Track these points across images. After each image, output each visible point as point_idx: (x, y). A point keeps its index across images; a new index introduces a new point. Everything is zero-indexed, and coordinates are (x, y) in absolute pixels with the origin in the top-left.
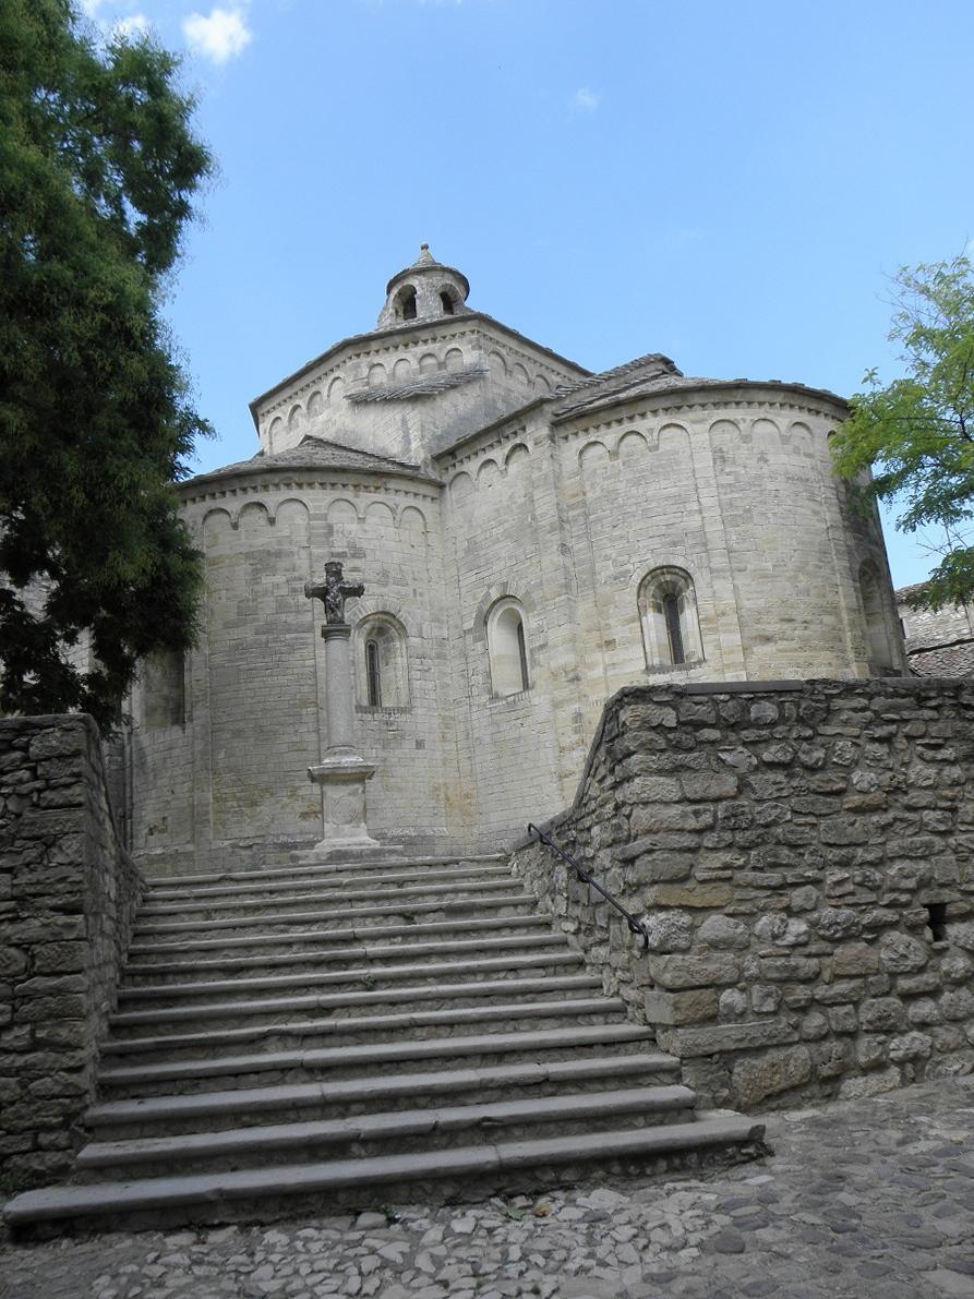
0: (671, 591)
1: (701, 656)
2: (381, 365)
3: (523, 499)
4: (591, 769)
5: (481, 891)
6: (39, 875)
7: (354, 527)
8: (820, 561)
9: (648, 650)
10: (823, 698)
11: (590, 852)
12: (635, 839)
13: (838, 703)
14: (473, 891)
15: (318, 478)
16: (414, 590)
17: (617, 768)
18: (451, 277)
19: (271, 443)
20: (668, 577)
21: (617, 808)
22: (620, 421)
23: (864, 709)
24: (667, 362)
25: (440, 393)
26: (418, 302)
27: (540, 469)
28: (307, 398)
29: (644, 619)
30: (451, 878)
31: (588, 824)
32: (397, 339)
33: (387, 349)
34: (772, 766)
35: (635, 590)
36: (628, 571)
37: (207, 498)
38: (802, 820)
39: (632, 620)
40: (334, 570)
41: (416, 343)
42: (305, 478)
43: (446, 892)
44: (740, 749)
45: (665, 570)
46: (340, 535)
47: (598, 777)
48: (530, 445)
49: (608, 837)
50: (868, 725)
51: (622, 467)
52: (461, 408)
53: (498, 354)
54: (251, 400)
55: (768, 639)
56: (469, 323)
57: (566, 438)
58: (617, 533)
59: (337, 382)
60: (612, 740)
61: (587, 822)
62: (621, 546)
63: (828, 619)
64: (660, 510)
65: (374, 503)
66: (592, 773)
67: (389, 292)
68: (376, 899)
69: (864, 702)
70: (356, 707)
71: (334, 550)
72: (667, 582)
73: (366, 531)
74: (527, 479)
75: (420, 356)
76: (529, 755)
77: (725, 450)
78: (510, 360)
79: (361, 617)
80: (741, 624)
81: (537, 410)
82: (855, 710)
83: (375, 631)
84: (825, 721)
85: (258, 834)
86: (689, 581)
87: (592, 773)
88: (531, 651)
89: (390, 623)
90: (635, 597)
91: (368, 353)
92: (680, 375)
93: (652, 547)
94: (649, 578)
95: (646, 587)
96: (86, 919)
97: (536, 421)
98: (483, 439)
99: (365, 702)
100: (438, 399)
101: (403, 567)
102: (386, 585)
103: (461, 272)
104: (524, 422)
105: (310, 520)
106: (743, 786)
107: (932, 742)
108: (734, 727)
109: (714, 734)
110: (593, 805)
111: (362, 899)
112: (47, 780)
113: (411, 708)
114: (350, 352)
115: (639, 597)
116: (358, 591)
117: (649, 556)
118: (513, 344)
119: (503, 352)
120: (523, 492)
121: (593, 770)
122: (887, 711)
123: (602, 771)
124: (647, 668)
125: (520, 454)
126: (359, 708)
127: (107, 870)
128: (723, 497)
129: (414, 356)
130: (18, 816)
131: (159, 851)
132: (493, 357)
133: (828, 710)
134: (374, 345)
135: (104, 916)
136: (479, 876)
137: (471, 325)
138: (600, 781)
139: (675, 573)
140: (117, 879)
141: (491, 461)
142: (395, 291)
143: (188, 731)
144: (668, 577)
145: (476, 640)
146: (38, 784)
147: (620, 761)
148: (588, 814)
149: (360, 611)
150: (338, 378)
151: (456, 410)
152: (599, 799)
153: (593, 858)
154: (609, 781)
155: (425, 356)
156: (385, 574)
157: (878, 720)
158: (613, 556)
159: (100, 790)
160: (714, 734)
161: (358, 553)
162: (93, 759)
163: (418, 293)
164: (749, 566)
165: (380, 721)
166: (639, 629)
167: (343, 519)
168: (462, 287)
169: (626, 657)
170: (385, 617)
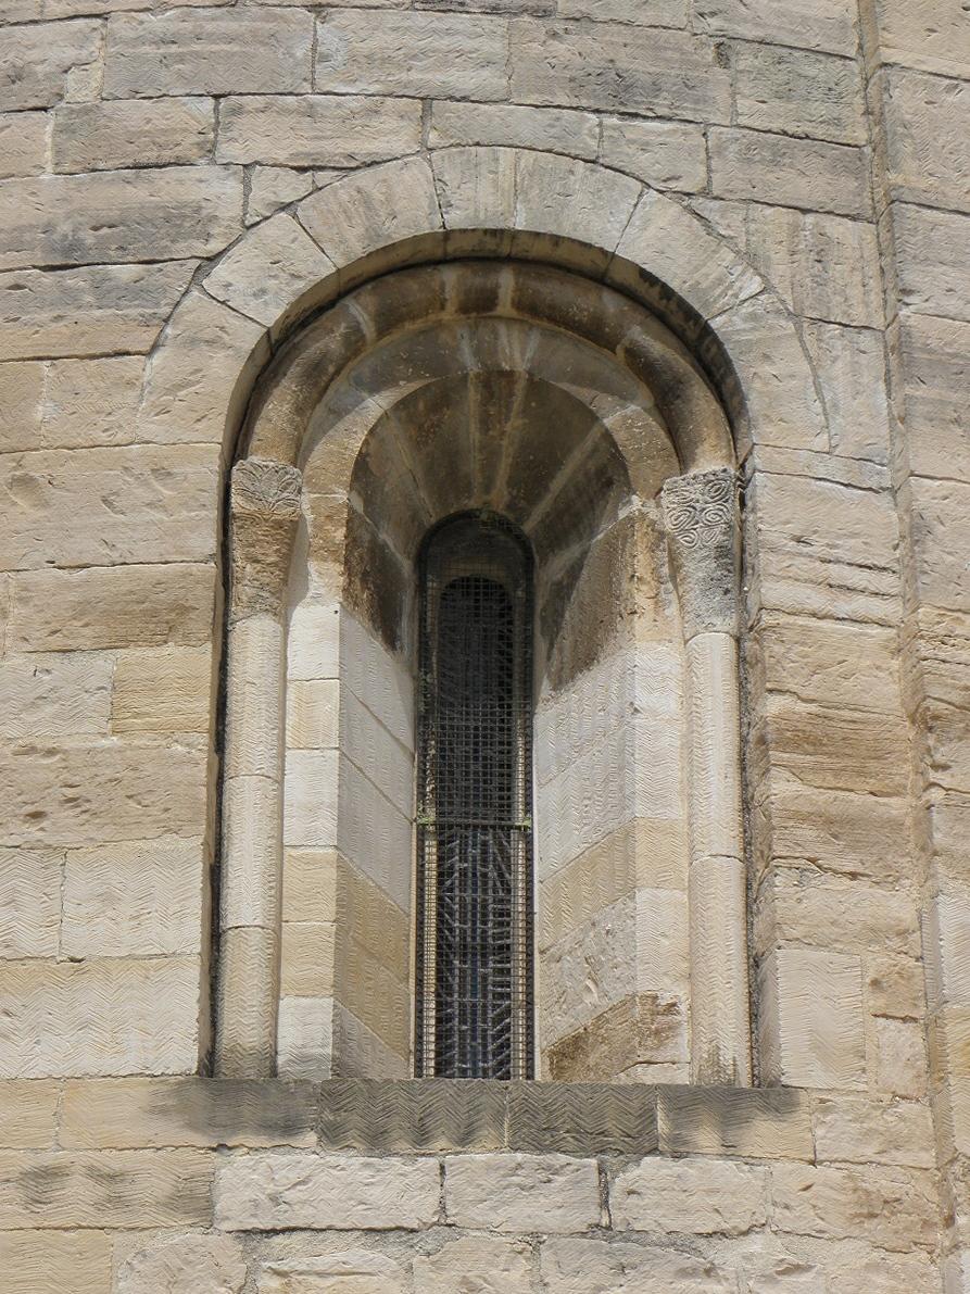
0: (500, 497)
1: (734, 1049)
9: (245, 904)
20: (518, 350)
29: (253, 635)
35: (224, 373)
36: (188, 219)
45: (506, 282)
72: (496, 381)
86: (701, 403)
90: (213, 434)
94: (360, 311)
95: (319, 381)
115: (237, 445)
117: (392, 134)
124: (210, 1064)
144: (518, 350)
158: (81, 89)
166: (204, 706)
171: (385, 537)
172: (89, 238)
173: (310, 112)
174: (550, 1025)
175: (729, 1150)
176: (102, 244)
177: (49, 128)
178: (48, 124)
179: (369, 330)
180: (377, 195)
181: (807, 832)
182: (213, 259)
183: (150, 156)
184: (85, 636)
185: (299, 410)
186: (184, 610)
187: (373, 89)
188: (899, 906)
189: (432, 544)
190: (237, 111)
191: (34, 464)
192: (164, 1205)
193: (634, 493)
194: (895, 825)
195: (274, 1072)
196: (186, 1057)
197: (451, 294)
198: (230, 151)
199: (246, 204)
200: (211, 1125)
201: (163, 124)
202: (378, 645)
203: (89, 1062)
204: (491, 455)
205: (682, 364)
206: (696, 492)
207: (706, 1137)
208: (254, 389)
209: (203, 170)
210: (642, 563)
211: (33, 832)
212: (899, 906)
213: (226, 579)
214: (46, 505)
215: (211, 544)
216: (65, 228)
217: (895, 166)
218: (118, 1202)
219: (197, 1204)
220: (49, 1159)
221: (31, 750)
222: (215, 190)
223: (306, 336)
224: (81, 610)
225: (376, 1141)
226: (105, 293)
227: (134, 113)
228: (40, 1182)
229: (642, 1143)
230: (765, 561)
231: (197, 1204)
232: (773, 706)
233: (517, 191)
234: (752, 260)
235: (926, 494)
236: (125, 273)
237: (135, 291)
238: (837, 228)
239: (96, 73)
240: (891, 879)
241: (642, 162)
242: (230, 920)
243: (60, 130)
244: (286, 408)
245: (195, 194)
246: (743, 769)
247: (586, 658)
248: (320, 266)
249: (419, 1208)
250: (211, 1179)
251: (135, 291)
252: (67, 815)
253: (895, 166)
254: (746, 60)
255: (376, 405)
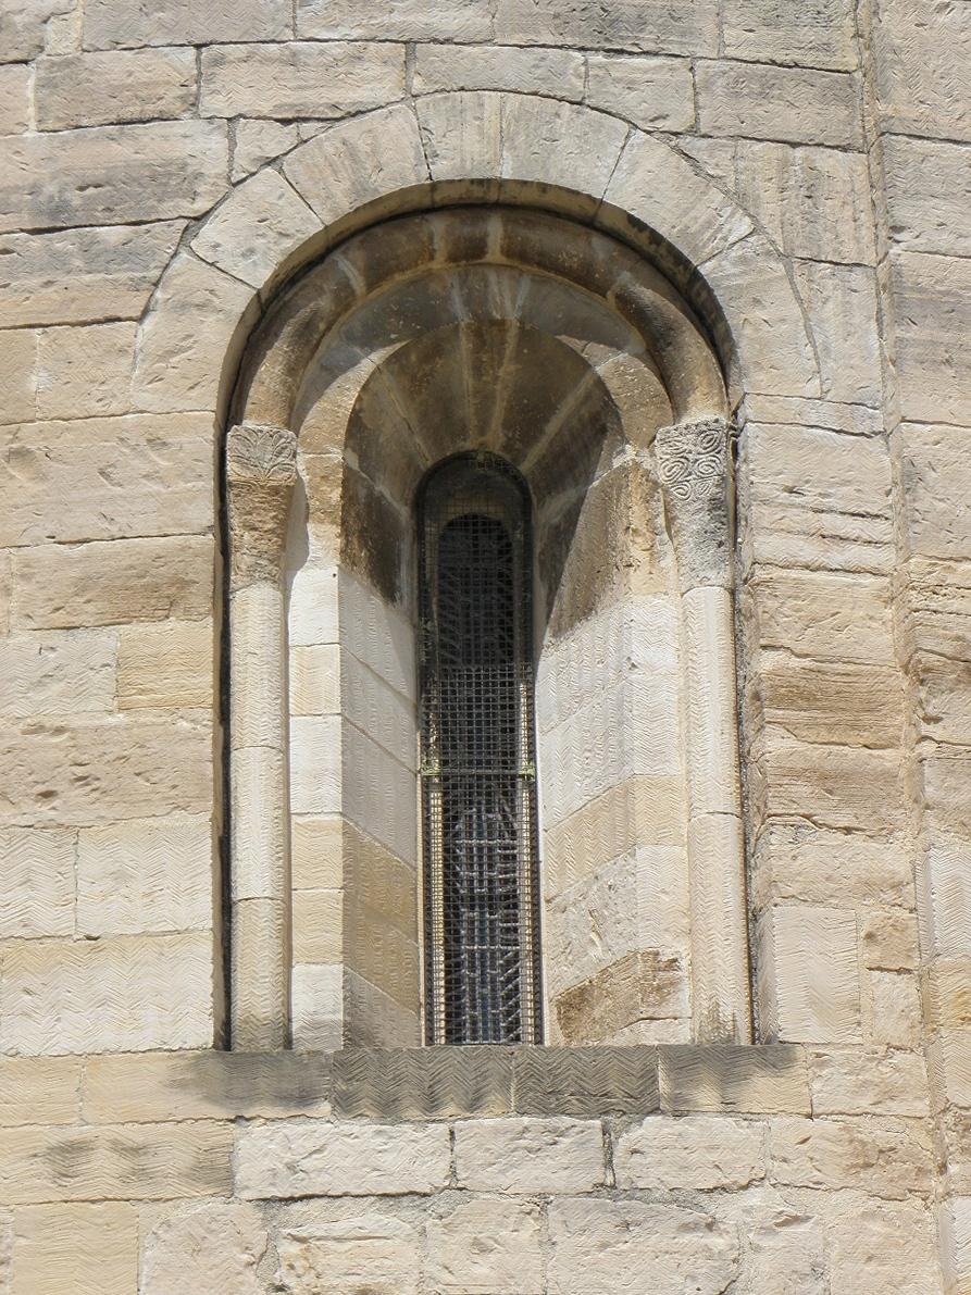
0: (496, 439)
1: (733, 1006)
9: (254, 875)
29: (252, 603)
35: (216, 337)
36: (174, 177)
39: (163, 598)
45: (495, 230)
72: (487, 330)
86: (693, 349)
90: (206, 402)
94: (349, 266)
95: (309, 340)
115: (231, 411)
117: (374, 82)
139: (586, 278)
144: (509, 298)
166: (207, 680)
169: (48, 919)
171: (383, 488)
172: (75, 198)
173: (293, 61)
174: (558, 976)
175: (729, 1107)
176: (88, 204)
177: (31, 82)
178: (30, 77)
179: (358, 283)
180: (363, 146)
181: (802, 789)
182: (200, 219)
183: (132, 111)
184: (88, 613)
185: (292, 370)
186: (184, 584)
187: (355, 34)
188: (893, 858)
189: (428, 489)
190: (219, 61)
191: (30, 438)
192: (187, 1176)
193: (628, 442)
194: (889, 777)
195: (288, 1042)
196: (203, 1032)
197: (440, 245)
198: (214, 103)
199: (231, 160)
200: (228, 1097)
201: (145, 77)
202: (377, 601)
203: (108, 1038)
204: (485, 399)
205: (672, 311)
206: (688, 443)
207: (706, 1096)
208: (245, 349)
209: (187, 124)
210: (636, 515)
211: (45, 811)
212: (893, 858)
213: (225, 548)
214: (44, 478)
215: (208, 516)
216: (51, 189)
217: (883, 96)
218: (142, 1174)
219: (218, 1174)
220: (74, 1133)
221: (39, 729)
223: (296, 294)
224: (82, 586)
225: (388, 1109)
226: (94, 256)
227: (116, 66)
228: (68, 1155)
229: (644, 1104)
230: (755, 513)
231: (218, 1174)
232: (766, 663)
233: (503, 138)
234: (742, 200)
235: (918, 439)
236: (113, 235)
237: (124, 254)
238: (828, 161)
239: (76, 21)
240: (885, 832)
241: (630, 102)
242: (239, 892)
243: (43, 84)
244: (278, 369)
245: (181, 150)
246: (739, 723)
247: (585, 609)
248: (307, 224)
249: (430, 1174)
250: (230, 1150)
251: (124, 254)
252: (77, 794)
253: (883, 96)
255: (369, 363)
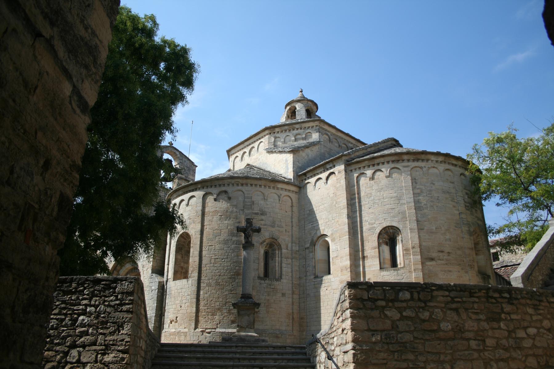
0: (392, 237)
2: (279, 137)
3: (333, 195)
4: (335, 313)
5: (293, 360)
6: (115, 337)
7: (262, 202)
8: (456, 227)
10: (429, 290)
11: (333, 348)
12: (348, 343)
13: (435, 293)
14: (289, 360)
15: (249, 181)
16: (286, 230)
17: (344, 314)
18: (311, 103)
19: (234, 166)
21: (343, 330)
22: (374, 165)
23: (447, 296)
24: (397, 141)
25: (302, 150)
26: (297, 113)
27: (340, 183)
28: (249, 149)
30: (282, 354)
31: (333, 336)
32: (286, 127)
33: (282, 131)
34: (407, 318)
35: (377, 235)
37: (205, 187)
38: (418, 341)
39: (376, 248)
40: (249, 221)
41: (294, 130)
42: (244, 181)
43: (278, 359)
44: (394, 310)
46: (257, 205)
47: (337, 317)
48: (336, 173)
49: (340, 342)
50: (447, 303)
51: (374, 184)
52: (310, 156)
53: (327, 135)
54: (228, 149)
55: (432, 259)
56: (316, 122)
57: (352, 170)
58: (371, 211)
59: (262, 143)
60: (343, 302)
61: (333, 335)
62: (372, 216)
63: (459, 252)
64: (389, 202)
65: (271, 193)
66: (335, 315)
67: (286, 108)
68: (250, 359)
69: (447, 293)
70: (258, 277)
71: (254, 212)
73: (267, 204)
74: (335, 186)
75: (295, 134)
76: (329, 303)
77: (417, 179)
78: (331, 137)
79: (263, 240)
80: (421, 252)
81: (340, 159)
82: (443, 296)
83: (268, 246)
84: (430, 301)
85: (213, 327)
87: (335, 315)
88: (333, 258)
89: (275, 243)
91: (275, 133)
92: (401, 146)
93: (384, 218)
96: (130, 356)
97: (340, 163)
98: (317, 169)
99: (262, 275)
100: (301, 152)
101: (282, 220)
102: (273, 227)
103: (315, 101)
104: (335, 164)
105: (245, 198)
106: (394, 326)
107: (475, 311)
108: (392, 301)
109: (383, 303)
110: (334, 329)
111: (244, 359)
112: (121, 301)
113: (281, 278)
114: (267, 132)
116: (258, 230)
118: (333, 131)
119: (329, 134)
120: (333, 192)
121: (336, 314)
122: (456, 297)
123: (339, 315)
125: (333, 176)
126: (259, 278)
127: (142, 338)
128: (415, 198)
129: (293, 134)
130: (110, 313)
131: (173, 330)
132: (325, 136)
133: (432, 297)
134: (277, 130)
135: (139, 356)
136: (293, 353)
137: (317, 123)
138: (338, 318)
139: (395, 229)
140: (146, 342)
141: (320, 179)
142: (288, 108)
143: (190, 282)
145: (310, 252)
146: (117, 302)
147: (345, 311)
148: (333, 332)
149: (263, 237)
150: (262, 142)
151: (308, 157)
152: (337, 326)
153: (334, 350)
154: (341, 319)
155: (297, 135)
156: (274, 222)
157: (453, 301)
159: (141, 306)
160: (383, 303)
161: (263, 213)
162: (139, 295)
163: (297, 109)
164: (426, 228)
165: (267, 284)
167: (257, 197)
168: (315, 107)
170: (273, 240)
171: (387, 240)
222: (375, 225)
237: (373, 231)
242: (381, 261)
254: (400, 213)
